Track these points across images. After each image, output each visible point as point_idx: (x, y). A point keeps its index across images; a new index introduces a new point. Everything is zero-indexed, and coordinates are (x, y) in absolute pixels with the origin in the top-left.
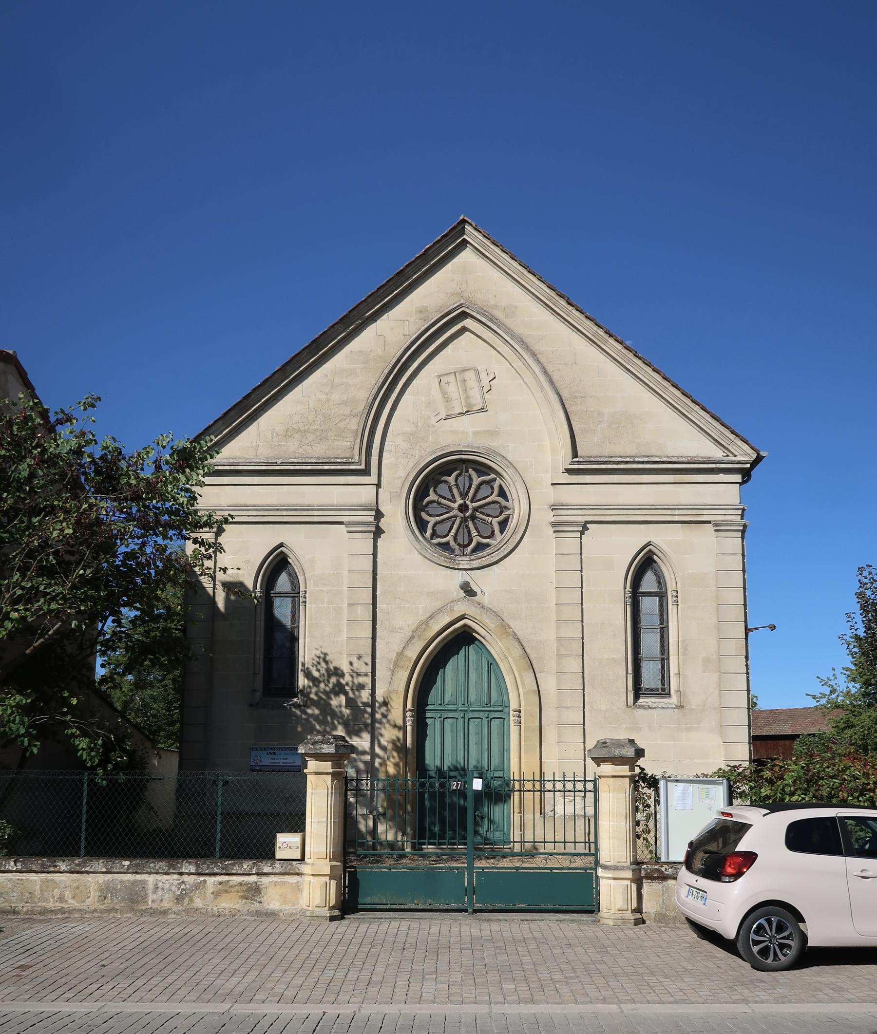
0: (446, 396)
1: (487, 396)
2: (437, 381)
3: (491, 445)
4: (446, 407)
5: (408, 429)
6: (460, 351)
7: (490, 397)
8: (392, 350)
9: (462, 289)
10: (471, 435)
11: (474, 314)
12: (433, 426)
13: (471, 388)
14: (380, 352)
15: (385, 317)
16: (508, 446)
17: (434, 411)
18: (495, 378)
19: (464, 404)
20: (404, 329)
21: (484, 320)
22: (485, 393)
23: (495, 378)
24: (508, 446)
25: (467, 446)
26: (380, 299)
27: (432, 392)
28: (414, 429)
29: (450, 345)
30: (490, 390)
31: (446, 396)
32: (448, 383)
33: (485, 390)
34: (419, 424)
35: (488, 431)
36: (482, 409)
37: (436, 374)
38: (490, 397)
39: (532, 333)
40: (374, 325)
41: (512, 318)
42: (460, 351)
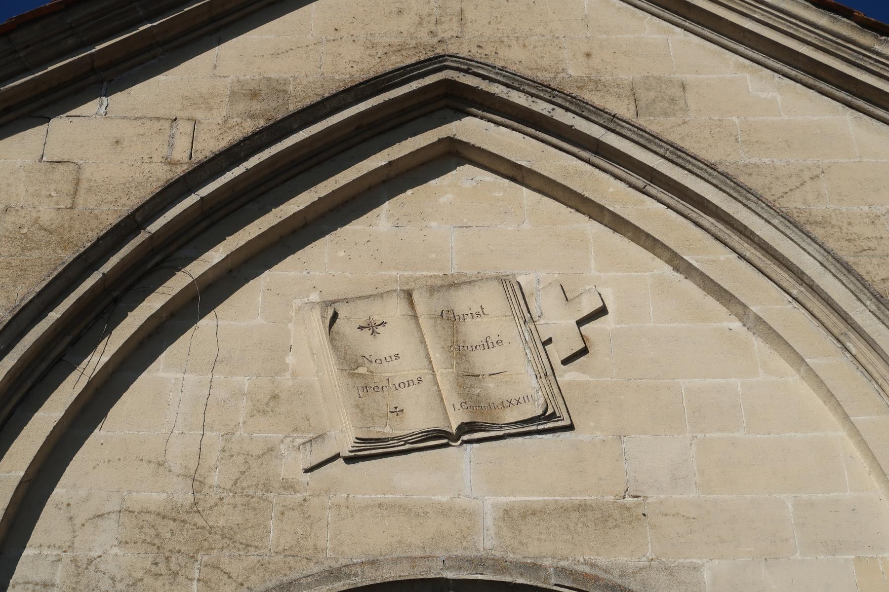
0: (362, 370)
1: (568, 376)
2: (317, 323)
3: (602, 561)
4: (360, 408)
5: (156, 498)
6: (434, 224)
7: (584, 378)
8: (105, 207)
9: (441, 35)
10: (489, 522)
11: (498, 90)
12: (289, 486)
13: (487, 344)
14: (47, 214)
15: (91, 107)
16: (696, 568)
17: (296, 430)
18: (602, 311)
19: (451, 398)
20: (171, 146)
21: (541, 107)
22: (557, 362)
23: (602, 311)
24: (696, 568)
25: (471, 561)
26: (71, 42)
27: (290, 359)
28: (185, 498)
29: (386, 205)
30: (584, 351)
31: (362, 370)
32: (372, 327)
33: (557, 353)
34: (215, 479)
35: (582, 508)
36: (545, 417)
37: (314, 297)
38: (584, 378)
39: (767, 161)
40: (40, 130)
41: (666, 114)
42: (434, 224)
